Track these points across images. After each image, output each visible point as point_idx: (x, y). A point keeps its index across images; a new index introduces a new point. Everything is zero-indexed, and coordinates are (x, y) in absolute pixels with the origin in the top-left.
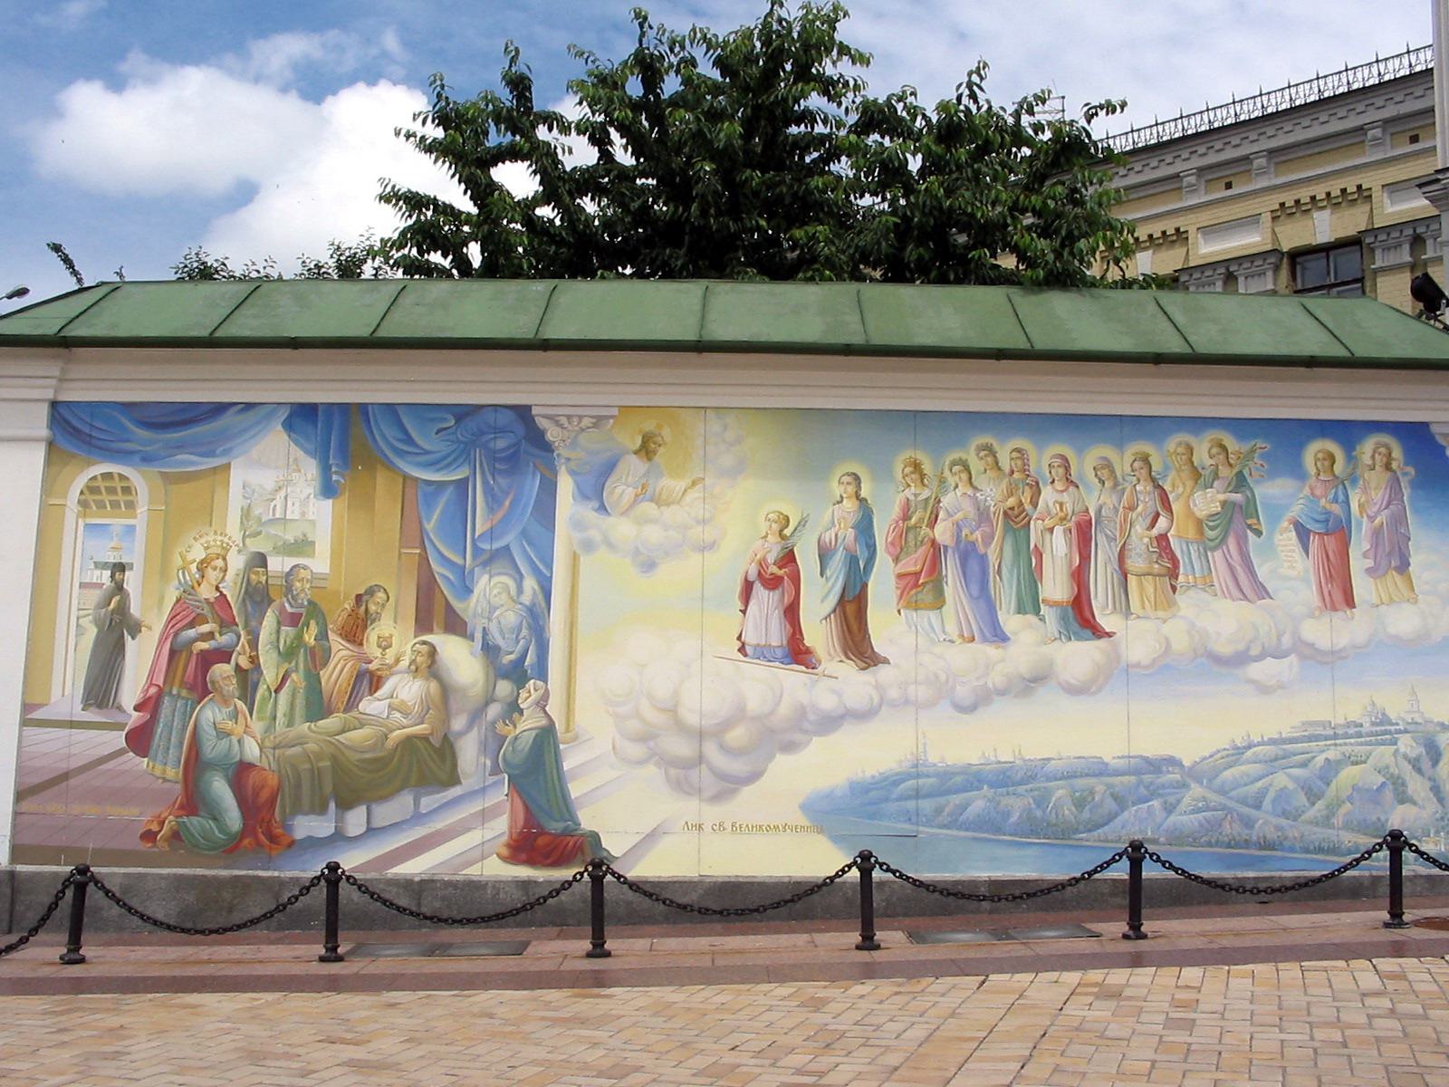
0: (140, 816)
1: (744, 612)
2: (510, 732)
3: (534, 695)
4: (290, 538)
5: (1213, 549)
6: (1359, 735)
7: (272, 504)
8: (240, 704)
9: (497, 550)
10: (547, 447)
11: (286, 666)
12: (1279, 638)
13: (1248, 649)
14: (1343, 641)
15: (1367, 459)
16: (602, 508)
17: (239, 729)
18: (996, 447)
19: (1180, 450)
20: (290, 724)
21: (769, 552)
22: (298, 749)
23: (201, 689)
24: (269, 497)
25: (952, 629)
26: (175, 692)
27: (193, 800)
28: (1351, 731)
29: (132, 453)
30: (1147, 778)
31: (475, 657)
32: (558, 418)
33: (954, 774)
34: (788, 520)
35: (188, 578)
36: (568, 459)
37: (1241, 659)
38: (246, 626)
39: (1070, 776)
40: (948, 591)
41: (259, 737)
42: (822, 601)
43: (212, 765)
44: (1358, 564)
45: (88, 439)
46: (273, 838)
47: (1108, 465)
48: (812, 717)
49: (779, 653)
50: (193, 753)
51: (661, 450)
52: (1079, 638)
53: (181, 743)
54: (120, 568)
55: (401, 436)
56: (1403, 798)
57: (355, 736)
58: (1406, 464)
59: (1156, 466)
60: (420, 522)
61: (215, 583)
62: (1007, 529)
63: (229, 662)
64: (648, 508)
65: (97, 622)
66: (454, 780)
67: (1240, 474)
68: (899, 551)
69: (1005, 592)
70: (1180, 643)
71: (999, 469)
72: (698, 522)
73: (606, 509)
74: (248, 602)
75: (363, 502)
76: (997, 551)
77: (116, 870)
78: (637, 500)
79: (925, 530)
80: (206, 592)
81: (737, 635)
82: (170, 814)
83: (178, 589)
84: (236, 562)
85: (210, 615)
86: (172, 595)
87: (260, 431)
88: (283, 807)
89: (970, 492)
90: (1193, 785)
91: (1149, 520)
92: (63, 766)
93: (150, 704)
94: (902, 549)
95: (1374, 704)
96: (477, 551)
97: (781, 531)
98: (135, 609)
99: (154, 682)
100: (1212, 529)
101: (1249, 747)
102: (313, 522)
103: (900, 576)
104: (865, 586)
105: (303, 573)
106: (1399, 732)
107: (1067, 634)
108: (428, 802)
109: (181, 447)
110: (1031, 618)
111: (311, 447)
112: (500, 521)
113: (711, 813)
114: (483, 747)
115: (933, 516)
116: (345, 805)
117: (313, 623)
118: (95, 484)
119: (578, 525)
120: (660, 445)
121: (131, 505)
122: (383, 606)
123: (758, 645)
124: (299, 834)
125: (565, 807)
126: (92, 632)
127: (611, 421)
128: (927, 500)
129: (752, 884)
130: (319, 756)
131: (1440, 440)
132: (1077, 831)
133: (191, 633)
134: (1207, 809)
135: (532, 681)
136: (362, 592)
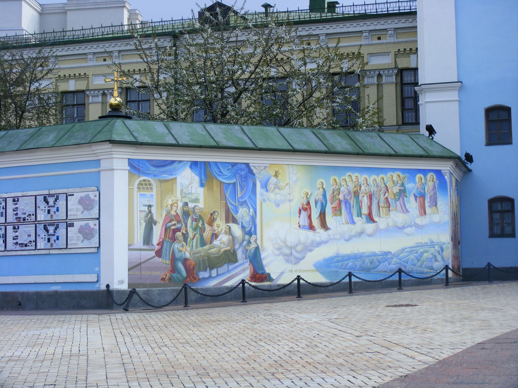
0: (161, 274)
1: (299, 217)
3: (254, 239)
4: (193, 197)
5: (397, 201)
6: (427, 246)
8: (184, 243)
10: (253, 174)
12: (411, 222)
13: (405, 225)
14: (424, 223)
15: (428, 179)
16: (267, 190)
17: (184, 250)
19: (390, 176)
20: (197, 248)
23: (174, 239)
25: (344, 221)
26: (167, 240)
27: (174, 269)
28: (426, 245)
29: (150, 174)
30: (385, 257)
33: (345, 256)
37: (403, 228)
38: (184, 222)
39: (369, 256)
41: (189, 251)
43: (177, 260)
44: (427, 205)
46: (195, 278)
47: (375, 180)
48: (315, 243)
49: (307, 227)
51: (279, 176)
52: (370, 223)
53: (170, 254)
54: (150, 206)
56: (436, 260)
57: (212, 250)
58: (437, 180)
59: (385, 181)
60: (225, 194)
62: (355, 196)
64: (277, 190)
65: (145, 221)
66: (236, 261)
67: (403, 182)
69: (355, 212)
70: (391, 224)
75: (210, 189)
76: (353, 202)
77: (155, 289)
78: (275, 188)
79: (337, 196)
80: (173, 213)
84: (180, 205)
86: (164, 214)
89: (347, 187)
90: (394, 258)
91: (384, 194)
92: (139, 261)
95: (430, 238)
96: (238, 201)
98: (155, 218)
100: (397, 196)
101: (405, 249)
102: (199, 194)
103: (332, 208)
104: (325, 210)
105: (197, 208)
106: (435, 245)
107: (368, 222)
108: (231, 267)
109: (163, 173)
110: (360, 218)
114: (243, 252)
116: (211, 269)
117: (200, 221)
119: (262, 195)
121: (151, 189)
124: (201, 277)
125: (262, 267)
126: (144, 224)
130: (204, 256)
131: (443, 174)
132: (371, 269)
133: (170, 224)
134: (397, 264)
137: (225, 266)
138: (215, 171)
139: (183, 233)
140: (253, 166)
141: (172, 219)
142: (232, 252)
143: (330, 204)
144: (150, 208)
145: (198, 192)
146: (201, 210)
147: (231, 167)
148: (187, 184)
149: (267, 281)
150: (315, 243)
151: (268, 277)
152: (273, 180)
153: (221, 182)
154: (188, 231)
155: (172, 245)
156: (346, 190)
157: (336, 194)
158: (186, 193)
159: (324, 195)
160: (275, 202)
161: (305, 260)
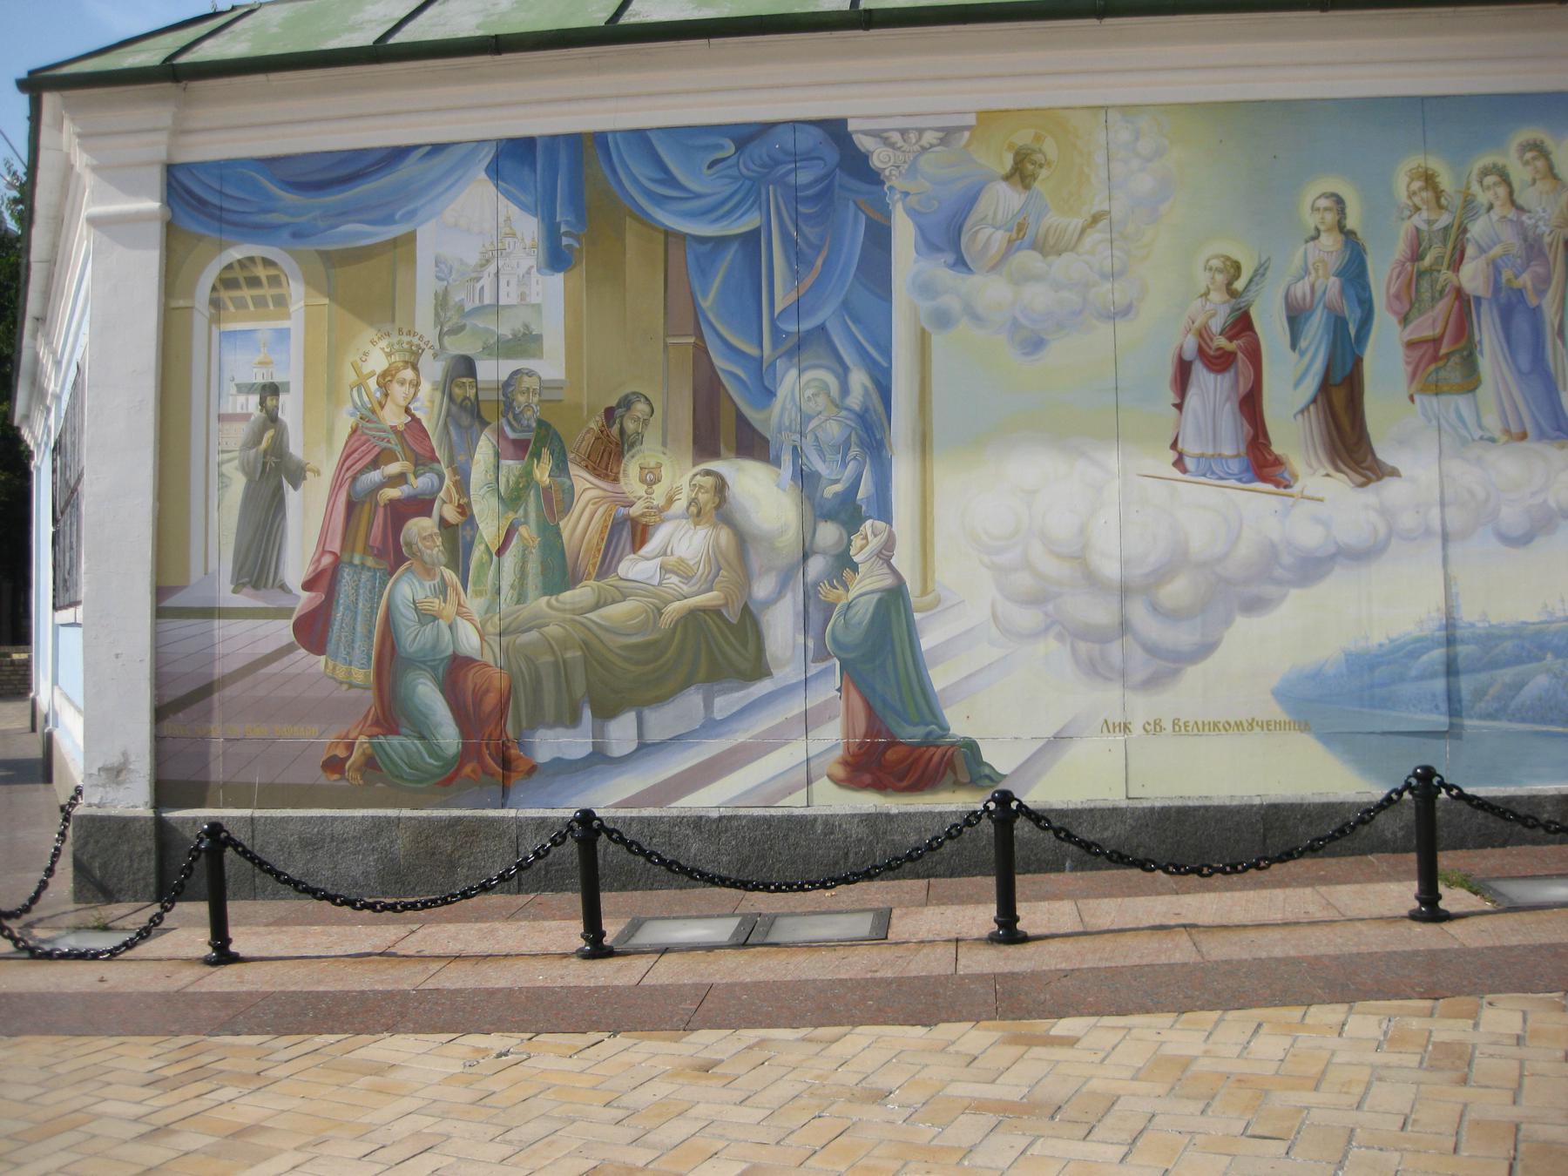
0: (322, 738)
1: (1179, 407)
2: (839, 598)
3: (874, 543)
4: (506, 331)
7: (478, 286)
8: (450, 575)
9: (808, 332)
11: (511, 516)
16: (961, 263)
17: (450, 609)
18: (1550, 143)
20: (521, 598)
21: (1213, 315)
22: (534, 635)
23: (394, 555)
24: (474, 275)
25: (1492, 422)
26: (357, 560)
31: (784, 490)
32: (885, 135)
34: (1237, 267)
35: (366, 398)
36: (906, 194)
38: (451, 462)
40: (1485, 364)
41: (477, 618)
42: (1297, 384)
43: (413, 663)
45: (218, 213)
48: (1287, 559)
49: (1235, 467)
50: (388, 645)
51: (1044, 173)
53: (370, 632)
54: (271, 390)
55: (661, 176)
61: (404, 404)
63: (429, 514)
64: (1028, 259)
65: (246, 469)
66: (759, 670)
68: (1408, 308)
71: (1555, 177)
72: (1104, 276)
73: (965, 264)
74: (452, 429)
78: (1011, 248)
79: (1445, 275)
80: (392, 417)
81: (1170, 442)
82: (360, 734)
83: (352, 415)
85: (398, 449)
86: (345, 423)
87: (457, 181)
88: (518, 722)
93: (323, 581)
94: (1412, 305)
96: (776, 331)
97: (1229, 284)
98: (295, 448)
99: (328, 548)
102: (537, 308)
103: (1411, 345)
104: (1358, 362)
105: (527, 382)
108: (725, 703)
109: (344, 214)
111: (528, 199)
112: (807, 291)
113: (1142, 708)
115: (1457, 256)
116: (605, 712)
118: (230, 275)
119: (925, 288)
120: (1041, 166)
121: (281, 302)
122: (646, 422)
123: (1202, 456)
124: (543, 755)
125: (924, 704)
127: (967, 134)
128: (1446, 229)
129: (1207, 808)
133: (375, 476)
135: (869, 523)
136: (613, 403)
137: (693, 699)
138: (635, 181)
139: (443, 523)
140: (866, 133)
141: (383, 450)
142: (734, 621)
143: (1393, 320)
144: (270, 402)
145: (534, 300)
146: (547, 395)
147: (730, 148)
148: (473, 259)
149: (957, 785)
150: (1287, 559)
151: (959, 761)
152: (1004, 199)
153: (668, 233)
154: (476, 509)
155: (384, 585)
156: (1509, 236)
157: (1438, 260)
158: (468, 307)
159: (1354, 272)
160: (1015, 325)
161: (1209, 664)
